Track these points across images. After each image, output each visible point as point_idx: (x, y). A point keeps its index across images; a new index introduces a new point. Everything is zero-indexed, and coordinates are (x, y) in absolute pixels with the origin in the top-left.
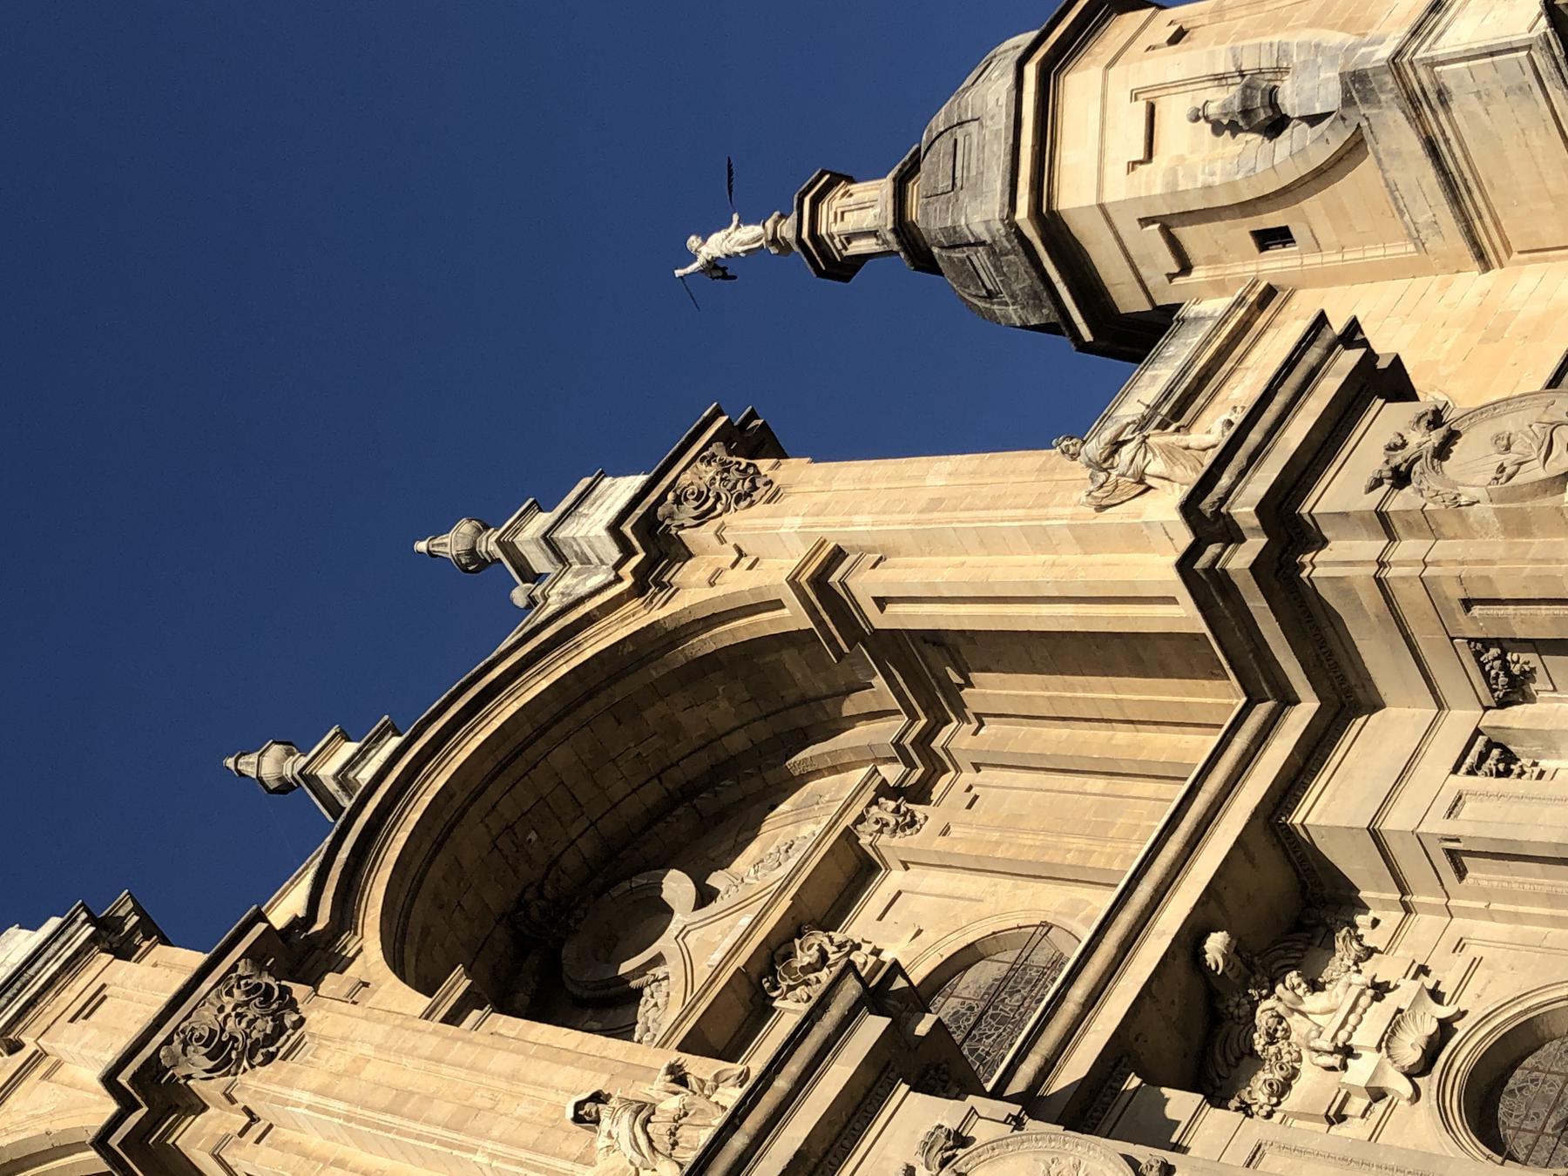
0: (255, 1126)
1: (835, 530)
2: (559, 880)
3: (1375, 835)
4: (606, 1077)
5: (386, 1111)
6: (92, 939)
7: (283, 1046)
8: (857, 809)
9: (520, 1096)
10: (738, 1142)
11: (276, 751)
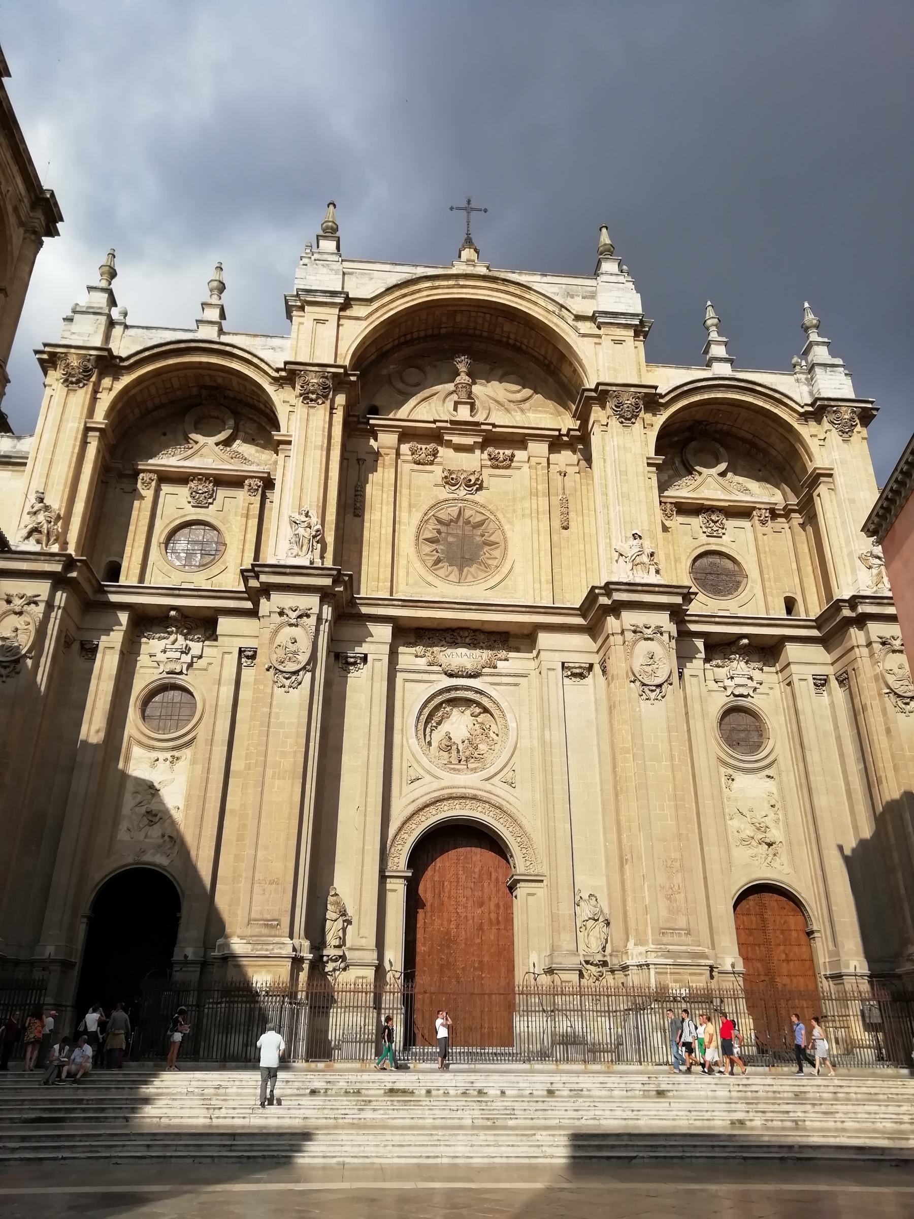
1: (836, 473)
3: (789, 664)
5: (620, 471)
6: (636, 325)
7: (628, 423)
8: (762, 506)
10: (640, 588)
11: (716, 321)
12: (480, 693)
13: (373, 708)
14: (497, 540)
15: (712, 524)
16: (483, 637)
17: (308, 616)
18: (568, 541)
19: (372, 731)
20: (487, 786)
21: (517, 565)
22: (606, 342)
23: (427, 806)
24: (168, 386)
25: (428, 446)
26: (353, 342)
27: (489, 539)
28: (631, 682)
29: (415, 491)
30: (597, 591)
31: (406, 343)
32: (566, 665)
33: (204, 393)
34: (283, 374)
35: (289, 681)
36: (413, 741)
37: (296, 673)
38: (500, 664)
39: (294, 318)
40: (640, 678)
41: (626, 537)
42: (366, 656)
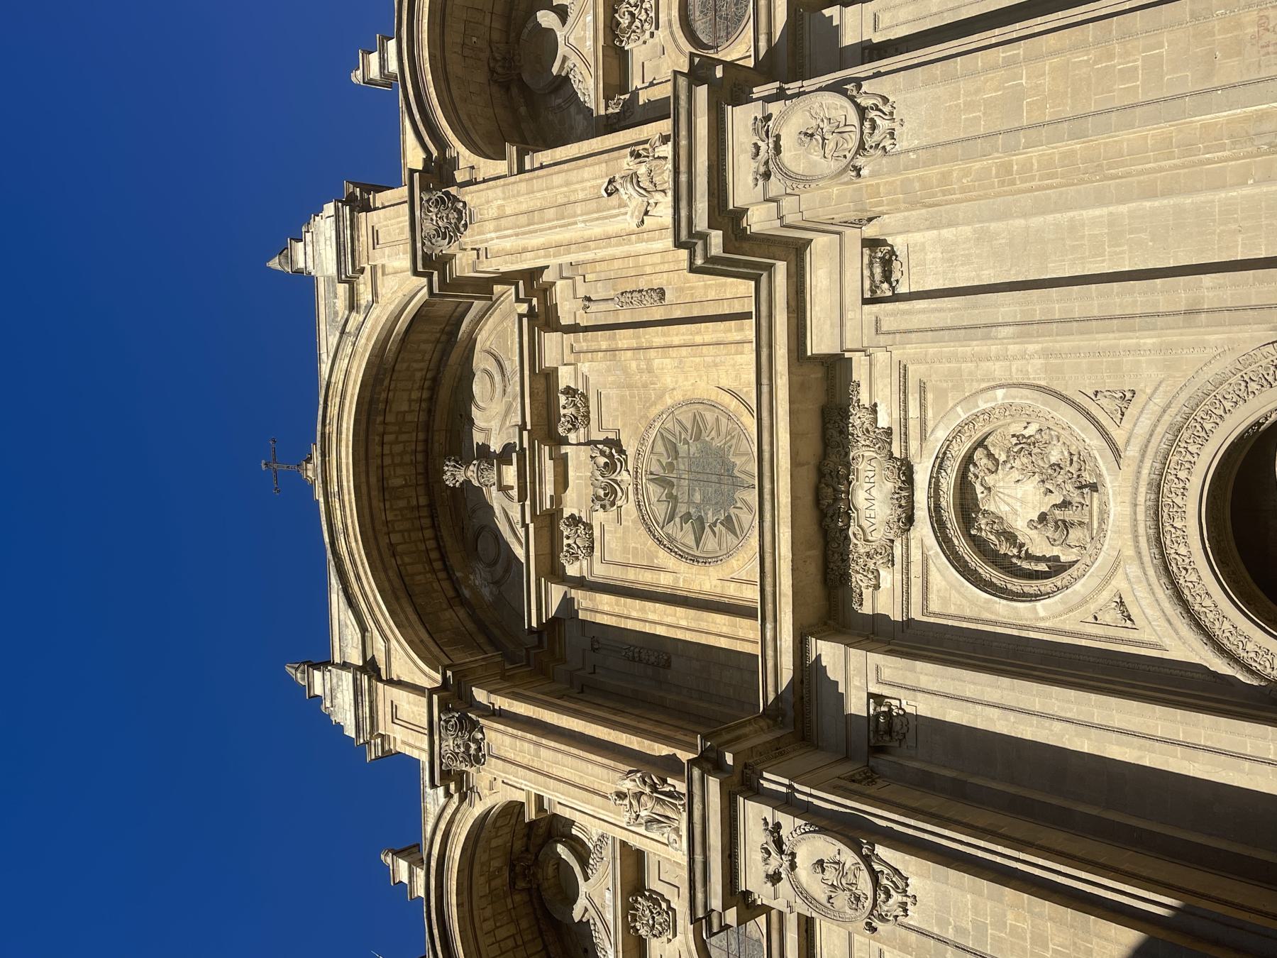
0: (480, 252)
2: (498, 48)
4: (604, 165)
5: (529, 225)
6: (351, 211)
7: (466, 218)
9: (576, 190)
10: (683, 178)
12: (943, 459)
13: (968, 694)
14: (691, 414)
15: (637, 23)
16: (833, 458)
17: (778, 826)
18: (681, 290)
19: (1013, 704)
20: (1132, 452)
21: (724, 383)
22: (380, 257)
23: (1179, 596)
24: (510, 943)
25: (565, 534)
26: (415, 663)
27: (690, 431)
28: (859, 175)
29: (630, 556)
30: (699, 262)
31: (443, 558)
32: (868, 295)
33: (521, 884)
34: (452, 786)
35: (892, 892)
36: (1040, 607)
37: (875, 876)
38: (883, 422)
39: (399, 750)
40: (849, 156)
41: (620, 206)
42: (870, 695)
